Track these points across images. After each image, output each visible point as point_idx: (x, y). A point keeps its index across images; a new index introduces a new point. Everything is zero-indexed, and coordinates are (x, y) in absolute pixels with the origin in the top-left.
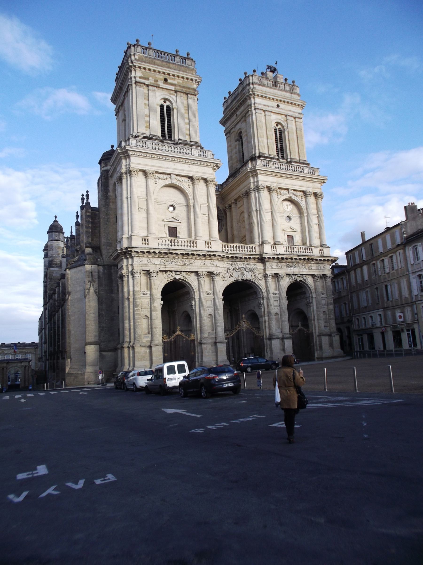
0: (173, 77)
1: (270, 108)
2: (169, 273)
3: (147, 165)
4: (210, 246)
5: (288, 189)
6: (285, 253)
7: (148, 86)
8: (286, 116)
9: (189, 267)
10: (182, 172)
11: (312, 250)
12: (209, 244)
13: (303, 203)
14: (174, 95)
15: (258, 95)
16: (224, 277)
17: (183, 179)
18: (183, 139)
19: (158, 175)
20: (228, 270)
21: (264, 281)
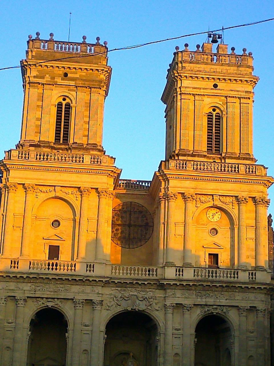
0: (74, 70)
1: (202, 90)
2: (39, 299)
3: (26, 179)
4: (92, 269)
5: (213, 195)
6: (196, 278)
7: (43, 84)
8: (226, 97)
9: (63, 294)
10: (68, 183)
11: (237, 274)
12: (92, 266)
13: (234, 213)
14: (75, 91)
15: (186, 77)
16: (109, 307)
17: (70, 190)
18: (78, 142)
19: (41, 188)
20: (115, 298)
21: (163, 311)
